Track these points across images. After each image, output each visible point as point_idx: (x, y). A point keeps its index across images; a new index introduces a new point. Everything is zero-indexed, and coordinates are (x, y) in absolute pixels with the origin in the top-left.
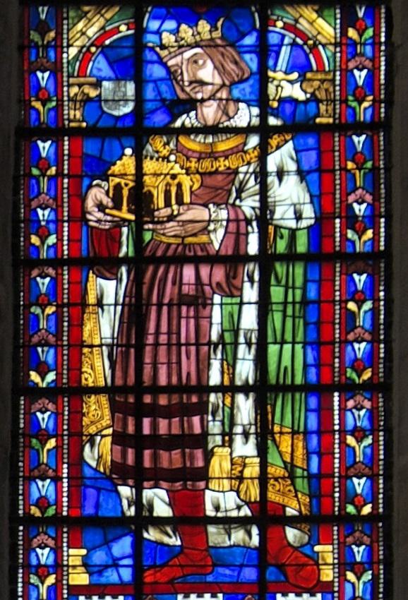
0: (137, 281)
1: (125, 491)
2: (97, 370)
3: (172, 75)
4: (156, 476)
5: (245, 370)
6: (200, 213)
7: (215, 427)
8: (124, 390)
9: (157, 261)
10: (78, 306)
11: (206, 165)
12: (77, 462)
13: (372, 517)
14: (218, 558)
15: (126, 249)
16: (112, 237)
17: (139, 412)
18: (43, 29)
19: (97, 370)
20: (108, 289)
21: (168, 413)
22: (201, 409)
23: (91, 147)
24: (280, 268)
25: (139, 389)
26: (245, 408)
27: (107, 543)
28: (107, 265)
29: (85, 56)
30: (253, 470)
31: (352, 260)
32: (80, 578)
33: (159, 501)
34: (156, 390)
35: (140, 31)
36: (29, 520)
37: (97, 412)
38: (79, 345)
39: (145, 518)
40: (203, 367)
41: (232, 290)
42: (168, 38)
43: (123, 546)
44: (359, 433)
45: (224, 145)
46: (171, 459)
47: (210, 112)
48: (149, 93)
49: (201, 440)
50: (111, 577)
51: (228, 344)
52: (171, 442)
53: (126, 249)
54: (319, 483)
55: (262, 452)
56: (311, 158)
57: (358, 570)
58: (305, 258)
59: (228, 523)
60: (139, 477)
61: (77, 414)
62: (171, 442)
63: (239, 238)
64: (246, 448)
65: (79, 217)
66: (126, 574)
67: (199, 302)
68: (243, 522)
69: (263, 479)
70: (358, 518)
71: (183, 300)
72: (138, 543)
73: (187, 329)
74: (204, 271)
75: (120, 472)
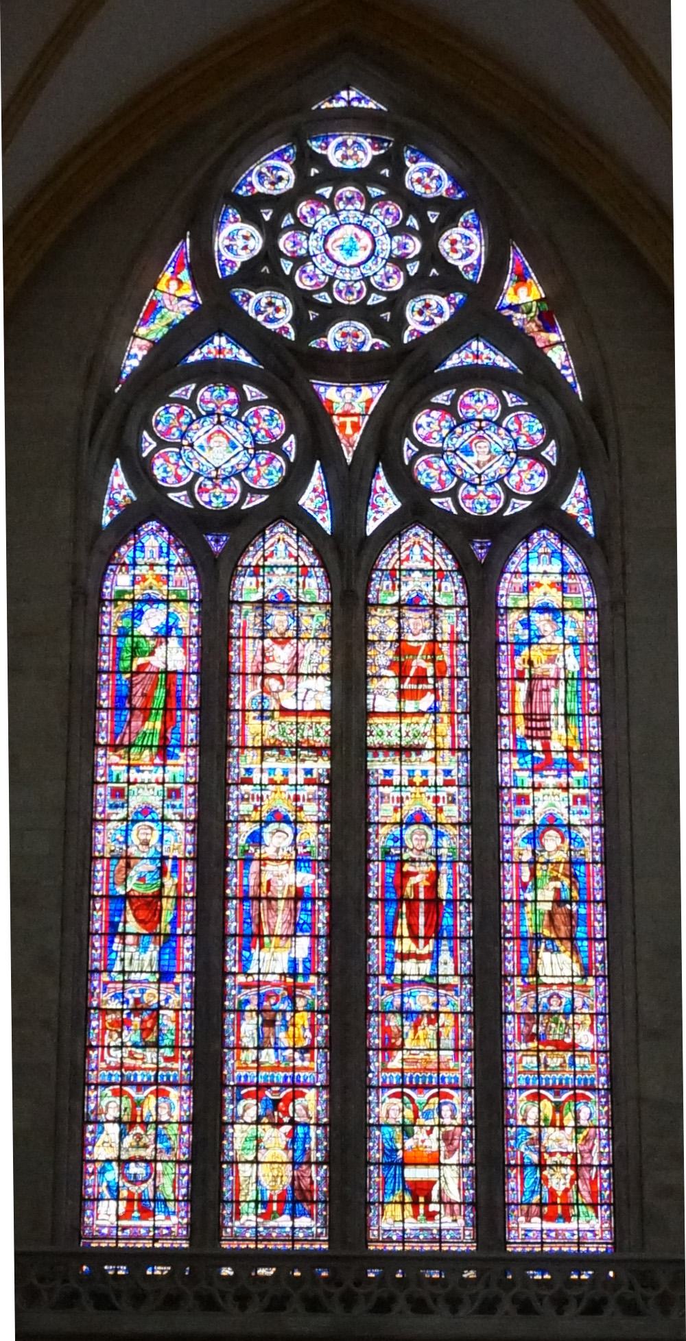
0: (530, 684)
1: (529, 742)
2: (520, 709)
3: (538, 629)
4: (537, 738)
5: (561, 710)
6: (547, 666)
7: (553, 724)
8: (527, 714)
9: (535, 679)
10: (514, 691)
11: (549, 653)
12: (515, 734)
13: (598, 751)
14: (554, 762)
15: (527, 676)
16: (522, 672)
17: (532, 720)
18: (502, 615)
19: (520, 709)
20: (522, 688)
21: (540, 721)
22: (549, 720)
23: (516, 647)
24: (570, 681)
25: (531, 714)
26: (561, 719)
27: (524, 756)
28: (521, 679)
29: (514, 623)
30: (564, 737)
31: (589, 680)
32: (517, 767)
33: (538, 745)
34: (536, 714)
35: (529, 617)
36: (501, 750)
37: (520, 721)
38: (514, 701)
39: (533, 751)
40: (549, 708)
41: (556, 687)
42: (537, 619)
43: (529, 758)
44: (594, 727)
45: (553, 647)
46: (541, 734)
47: (549, 639)
48: (532, 633)
49: (549, 729)
50: (525, 766)
51: (557, 703)
52: (540, 729)
53: (527, 676)
54: (583, 742)
55: (567, 732)
56: (578, 652)
57: (595, 765)
58: (578, 679)
59: (557, 752)
60: (532, 738)
61: (514, 721)
62: (540, 729)
63: (558, 673)
64: (562, 731)
65: (513, 667)
66: (530, 766)
67: (547, 690)
68: (562, 752)
69: (567, 740)
70: (593, 752)
71: (543, 690)
72: (533, 757)
73: (544, 698)
74: (549, 681)
75: (527, 737)
